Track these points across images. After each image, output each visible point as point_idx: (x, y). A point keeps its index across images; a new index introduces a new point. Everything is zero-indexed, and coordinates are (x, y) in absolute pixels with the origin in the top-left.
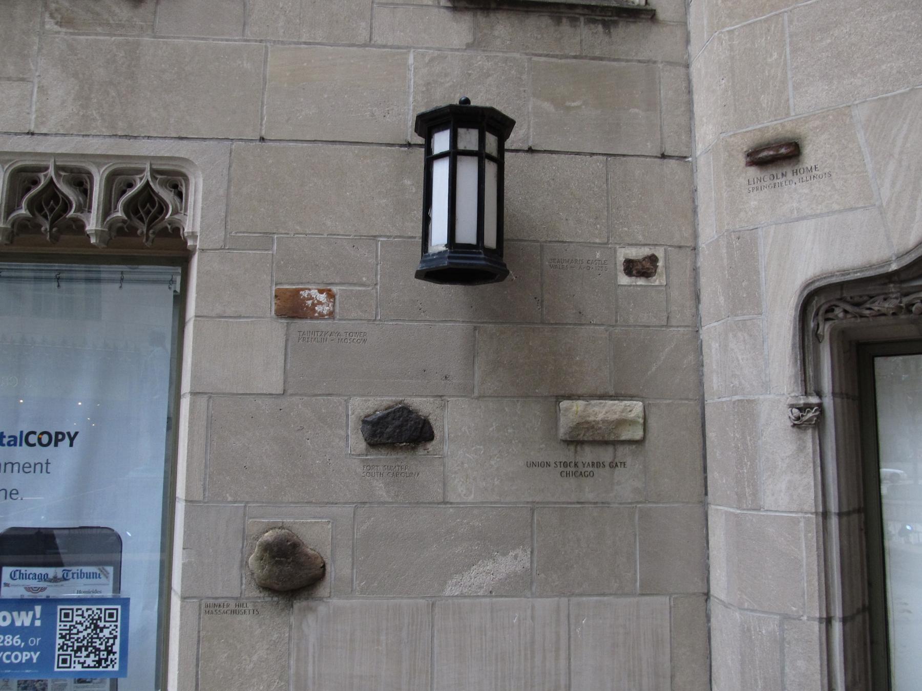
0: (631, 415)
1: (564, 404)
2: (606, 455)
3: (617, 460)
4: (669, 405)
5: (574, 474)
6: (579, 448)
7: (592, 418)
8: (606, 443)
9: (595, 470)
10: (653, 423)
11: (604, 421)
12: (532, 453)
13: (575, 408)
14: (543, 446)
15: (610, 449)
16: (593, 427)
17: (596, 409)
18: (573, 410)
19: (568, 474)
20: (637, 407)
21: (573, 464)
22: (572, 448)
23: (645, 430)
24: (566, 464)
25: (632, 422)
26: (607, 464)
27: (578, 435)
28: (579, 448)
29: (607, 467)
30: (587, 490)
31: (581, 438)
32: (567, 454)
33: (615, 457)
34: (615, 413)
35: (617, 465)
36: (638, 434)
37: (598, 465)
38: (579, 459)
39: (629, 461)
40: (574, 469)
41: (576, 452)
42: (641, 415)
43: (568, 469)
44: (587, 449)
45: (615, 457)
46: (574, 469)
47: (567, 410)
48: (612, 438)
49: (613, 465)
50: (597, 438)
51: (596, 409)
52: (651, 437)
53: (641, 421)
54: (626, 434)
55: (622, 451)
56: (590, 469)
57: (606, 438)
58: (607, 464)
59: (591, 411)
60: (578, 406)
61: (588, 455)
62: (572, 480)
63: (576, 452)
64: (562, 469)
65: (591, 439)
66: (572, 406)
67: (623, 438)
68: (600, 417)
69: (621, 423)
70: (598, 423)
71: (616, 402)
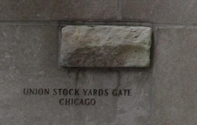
0: (137, 41)
1: (66, 29)
2: (109, 82)
3: (120, 88)
4: (179, 30)
5: (74, 102)
6: (80, 75)
7: (93, 45)
8: (110, 70)
9: (97, 98)
10: (162, 50)
11: (106, 47)
12: (30, 80)
13: (76, 33)
14: (41, 73)
15: (115, 76)
16: (93, 53)
17: (99, 35)
18: (75, 35)
19: (67, 102)
20: (145, 32)
21: (73, 92)
22: (73, 75)
23: (152, 57)
24: (65, 92)
25: (138, 49)
26: (110, 92)
27: (78, 61)
28: (80, 75)
29: (110, 95)
30: (87, 118)
31: (81, 64)
32: (68, 81)
33: (119, 84)
34: (119, 38)
35: (121, 93)
36: (144, 60)
37: (100, 92)
38: (80, 86)
39: (134, 89)
40: (73, 97)
41: (77, 79)
42: (148, 40)
43: (69, 97)
44: (90, 76)
45: (119, 84)
46: (73, 97)
47: (67, 35)
48: (115, 64)
49: (117, 93)
50: (98, 65)
51: (99, 35)
52: (159, 64)
53: (147, 47)
54: (130, 62)
55: (126, 78)
56: (91, 97)
57: (108, 65)
58: (110, 92)
59: (93, 37)
60: (80, 31)
61: (90, 82)
62: (72, 108)
63: (77, 79)
64: (62, 96)
65: (91, 65)
66: (74, 31)
67: (128, 64)
68: (102, 43)
69: (125, 49)
70: (99, 49)
71: (122, 27)
